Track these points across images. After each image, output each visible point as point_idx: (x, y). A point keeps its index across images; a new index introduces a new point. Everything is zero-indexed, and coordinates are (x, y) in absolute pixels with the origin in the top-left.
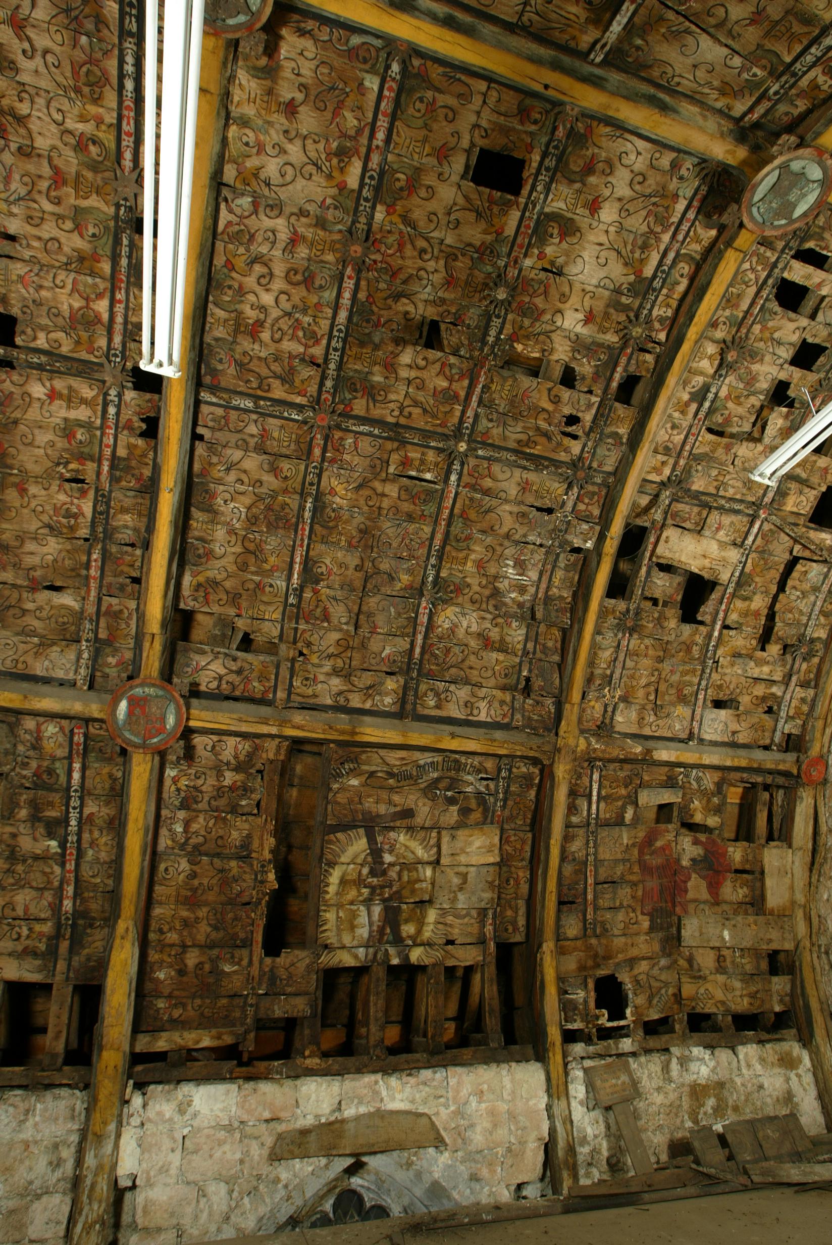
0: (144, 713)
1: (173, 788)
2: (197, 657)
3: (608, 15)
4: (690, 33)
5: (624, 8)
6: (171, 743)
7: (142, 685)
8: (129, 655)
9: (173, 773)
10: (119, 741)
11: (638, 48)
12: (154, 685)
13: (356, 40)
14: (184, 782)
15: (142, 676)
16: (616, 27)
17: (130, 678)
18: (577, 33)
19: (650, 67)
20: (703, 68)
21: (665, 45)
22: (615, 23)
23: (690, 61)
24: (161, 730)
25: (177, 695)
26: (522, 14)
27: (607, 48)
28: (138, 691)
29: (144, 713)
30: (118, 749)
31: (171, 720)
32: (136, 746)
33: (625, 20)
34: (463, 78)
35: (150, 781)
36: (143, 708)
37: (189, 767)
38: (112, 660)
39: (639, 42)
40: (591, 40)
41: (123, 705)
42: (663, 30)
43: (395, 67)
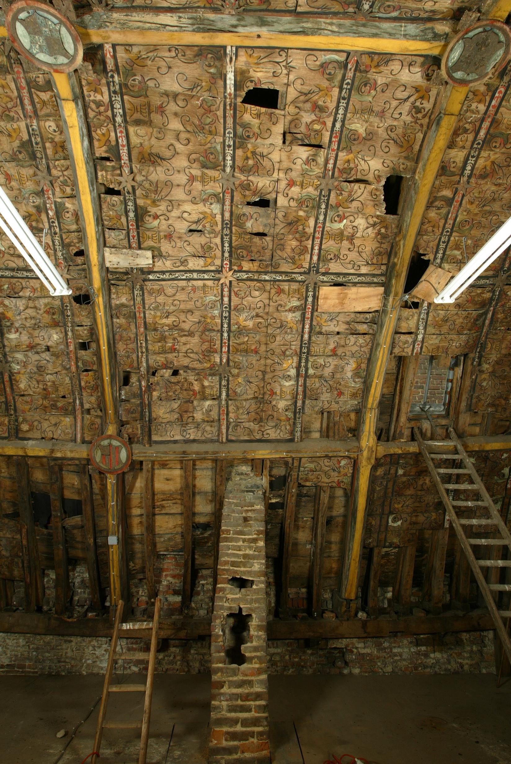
3: (238, 79)
4: (189, 89)
5: (233, 89)
11: (210, 66)
13: (395, 14)
16: (230, 76)
18: (250, 60)
19: (195, 56)
20: (164, 70)
21: (196, 75)
22: (233, 78)
23: (175, 70)
26: (287, 56)
27: (228, 59)
33: (228, 82)
34: (316, 10)
39: (212, 70)
40: (239, 58)
42: (204, 84)
43: (366, 7)
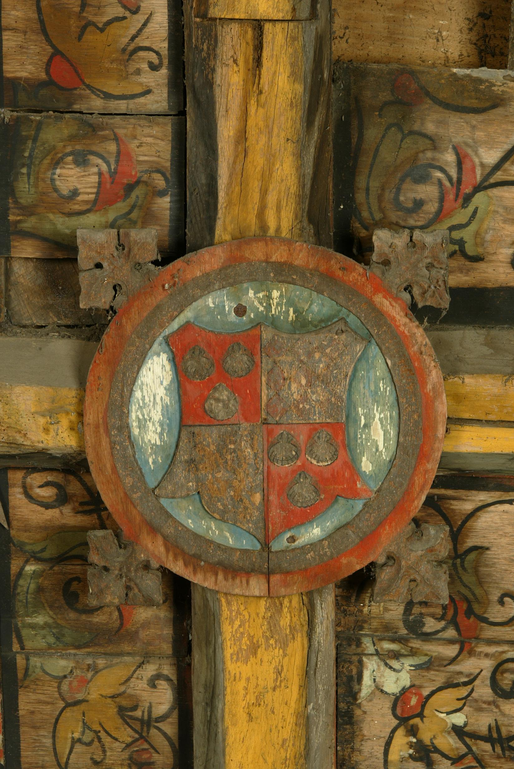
0: (250, 407)
1: (401, 745)
2: (457, 129)
6: (389, 540)
7: (230, 276)
8: (152, 147)
9: (395, 680)
10: (154, 549)
12: (283, 272)
14: (444, 719)
15: (223, 230)
17: (175, 249)
24: (340, 482)
25: (396, 313)
28: (215, 307)
29: (250, 407)
30: (152, 584)
31: (377, 435)
32: (233, 568)
35: (305, 722)
36: (245, 388)
37: (466, 645)
38: (77, 179)
41: (155, 377)
